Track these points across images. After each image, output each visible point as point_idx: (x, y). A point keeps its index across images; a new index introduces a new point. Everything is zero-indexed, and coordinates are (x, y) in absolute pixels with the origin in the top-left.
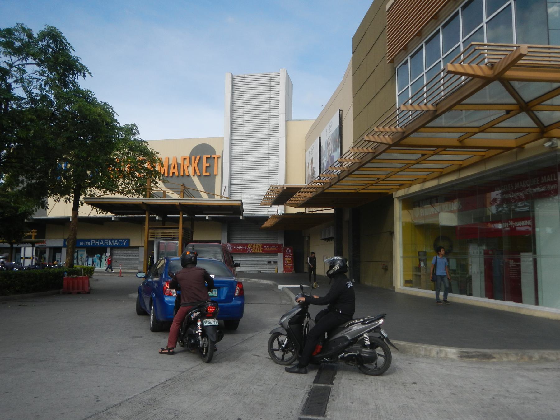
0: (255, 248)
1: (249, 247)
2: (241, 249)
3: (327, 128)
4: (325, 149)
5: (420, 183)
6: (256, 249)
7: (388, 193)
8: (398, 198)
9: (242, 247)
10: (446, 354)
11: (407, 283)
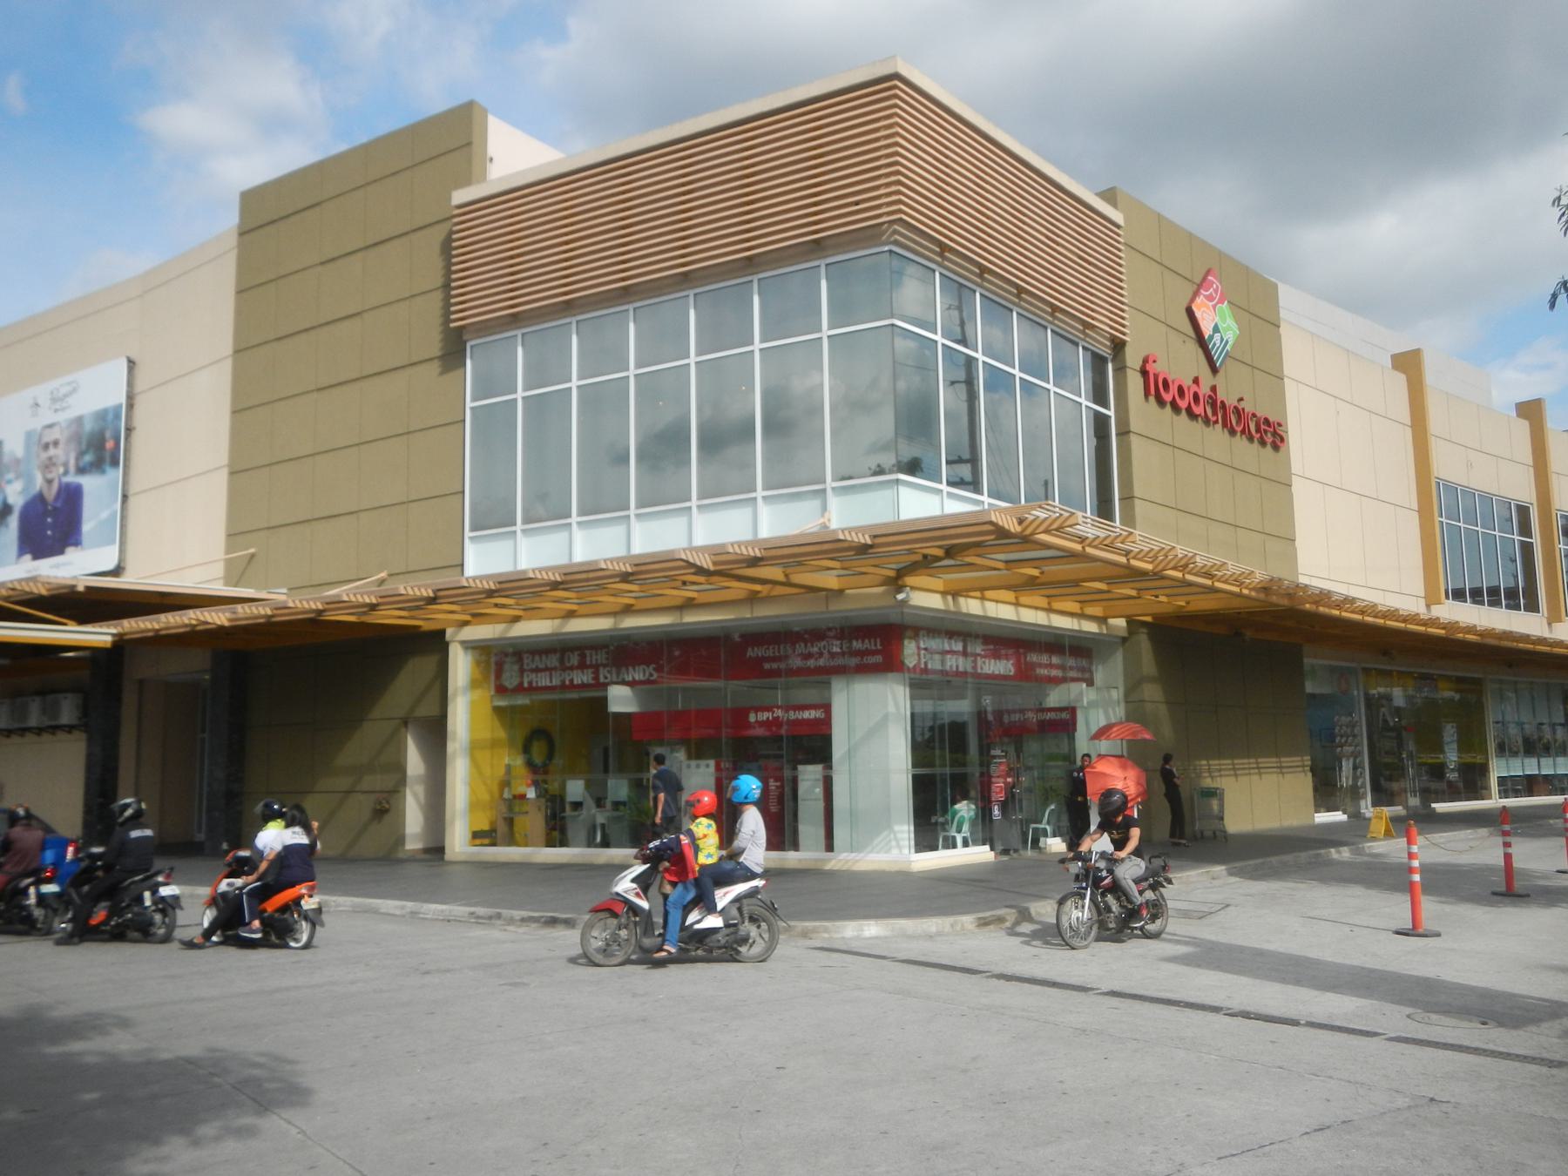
3: (41, 392)
5: (553, 618)
7: (420, 627)
10: (963, 925)
11: (476, 835)
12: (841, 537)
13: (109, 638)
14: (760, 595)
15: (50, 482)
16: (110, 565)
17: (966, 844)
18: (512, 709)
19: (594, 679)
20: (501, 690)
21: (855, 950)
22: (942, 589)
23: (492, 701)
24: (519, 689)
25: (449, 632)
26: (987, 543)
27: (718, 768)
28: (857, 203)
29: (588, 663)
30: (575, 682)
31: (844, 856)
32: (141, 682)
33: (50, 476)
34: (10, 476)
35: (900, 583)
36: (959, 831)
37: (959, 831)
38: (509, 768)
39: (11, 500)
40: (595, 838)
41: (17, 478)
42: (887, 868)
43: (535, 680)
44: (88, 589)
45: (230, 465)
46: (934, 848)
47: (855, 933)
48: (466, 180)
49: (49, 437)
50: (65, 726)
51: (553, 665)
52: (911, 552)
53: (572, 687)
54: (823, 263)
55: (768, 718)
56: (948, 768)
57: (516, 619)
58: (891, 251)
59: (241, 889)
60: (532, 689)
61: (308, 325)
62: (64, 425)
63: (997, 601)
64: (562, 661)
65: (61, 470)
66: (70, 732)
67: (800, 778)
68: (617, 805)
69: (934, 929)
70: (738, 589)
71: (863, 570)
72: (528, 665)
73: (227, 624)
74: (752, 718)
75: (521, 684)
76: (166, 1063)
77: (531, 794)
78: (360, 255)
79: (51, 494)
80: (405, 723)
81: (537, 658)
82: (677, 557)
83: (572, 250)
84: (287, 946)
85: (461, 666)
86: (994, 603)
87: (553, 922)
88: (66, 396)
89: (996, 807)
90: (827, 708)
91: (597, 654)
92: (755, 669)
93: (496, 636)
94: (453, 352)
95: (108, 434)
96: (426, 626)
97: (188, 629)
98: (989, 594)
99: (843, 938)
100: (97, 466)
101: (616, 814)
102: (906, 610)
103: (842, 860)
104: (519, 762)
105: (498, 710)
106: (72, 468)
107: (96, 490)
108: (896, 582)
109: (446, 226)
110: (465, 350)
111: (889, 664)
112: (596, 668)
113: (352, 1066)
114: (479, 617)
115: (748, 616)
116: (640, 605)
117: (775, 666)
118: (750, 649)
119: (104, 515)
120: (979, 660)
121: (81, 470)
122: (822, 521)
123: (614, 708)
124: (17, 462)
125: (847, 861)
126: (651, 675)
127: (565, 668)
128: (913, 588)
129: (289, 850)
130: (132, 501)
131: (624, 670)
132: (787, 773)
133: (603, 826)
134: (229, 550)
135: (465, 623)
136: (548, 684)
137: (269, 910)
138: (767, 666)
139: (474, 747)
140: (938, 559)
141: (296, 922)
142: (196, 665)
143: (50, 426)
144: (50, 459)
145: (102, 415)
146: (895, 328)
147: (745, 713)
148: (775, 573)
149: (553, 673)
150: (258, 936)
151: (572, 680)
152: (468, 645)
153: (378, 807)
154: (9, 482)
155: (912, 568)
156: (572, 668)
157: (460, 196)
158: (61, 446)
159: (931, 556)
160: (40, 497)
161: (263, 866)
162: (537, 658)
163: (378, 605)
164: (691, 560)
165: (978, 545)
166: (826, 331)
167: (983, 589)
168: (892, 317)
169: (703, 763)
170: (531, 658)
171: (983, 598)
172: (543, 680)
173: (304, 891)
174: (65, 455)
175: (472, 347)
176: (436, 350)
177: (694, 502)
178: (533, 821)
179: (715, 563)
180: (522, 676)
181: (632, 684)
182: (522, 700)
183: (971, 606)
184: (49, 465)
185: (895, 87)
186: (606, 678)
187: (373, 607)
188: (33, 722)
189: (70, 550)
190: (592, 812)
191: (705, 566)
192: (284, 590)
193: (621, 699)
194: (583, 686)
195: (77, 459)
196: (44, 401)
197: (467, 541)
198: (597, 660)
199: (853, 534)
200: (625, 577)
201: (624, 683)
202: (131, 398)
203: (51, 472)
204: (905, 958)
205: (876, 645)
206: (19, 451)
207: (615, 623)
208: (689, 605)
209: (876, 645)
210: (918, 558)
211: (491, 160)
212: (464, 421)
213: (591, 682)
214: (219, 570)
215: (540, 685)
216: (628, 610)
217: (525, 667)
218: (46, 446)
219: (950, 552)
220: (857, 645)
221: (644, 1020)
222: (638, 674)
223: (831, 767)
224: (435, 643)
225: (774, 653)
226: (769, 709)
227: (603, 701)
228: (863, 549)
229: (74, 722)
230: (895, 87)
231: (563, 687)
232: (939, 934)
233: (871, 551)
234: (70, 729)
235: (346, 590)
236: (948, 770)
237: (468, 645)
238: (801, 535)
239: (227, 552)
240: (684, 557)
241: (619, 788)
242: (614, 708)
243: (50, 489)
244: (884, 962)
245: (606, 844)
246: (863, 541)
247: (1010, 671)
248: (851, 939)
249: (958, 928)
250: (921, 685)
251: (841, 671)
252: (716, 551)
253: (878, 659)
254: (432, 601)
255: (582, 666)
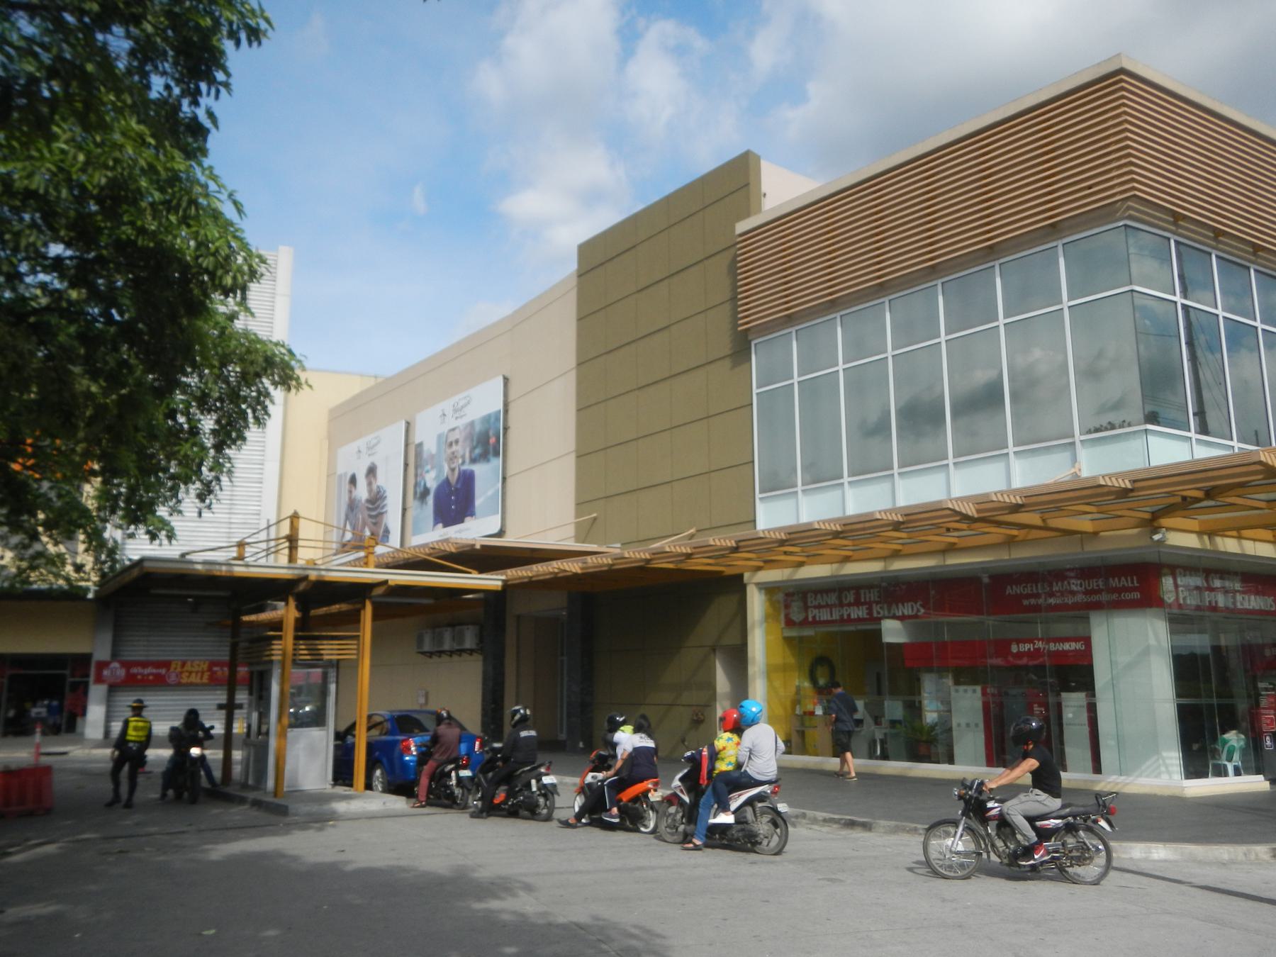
0: (190, 673)
1: (172, 670)
2: (149, 675)
3: (447, 405)
4: (434, 450)
5: (832, 563)
6: (194, 675)
8: (757, 584)
9: (154, 671)
10: (1257, 855)
12: (1102, 482)
13: (500, 583)
14: (1017, 539)
15: (453, 470)
16: (495, 529)
17: (1237, 772)
18: (801, 639)
19: (868, 614)
20: (789, 623)
21: (1146, 871)
22: (1197, 529)
23: (782, 632)
24: (805, 623)
25: (746, 576)
26: (1253, 483)
27: (984, 693)
28: (1090, 187)
29: (863, 600)
30: (852, 617)
31: (1113, 778)
32: (519, 617)
33: (453, 466)
34: (428, 467)
35: (1156, 524)
36: (1230, 760)
37: (1230, 760)
38: (798, 690)
39: (428, 485)
40: (875, 751)
41: (432, 468)
42: (1158, 792)
43: (818, 614)
44: (483, 546)
45: (577, 451)
46: (1204, 775)
47: (1143, 855)
48: (747, 214)
49: (452, 438)
50: (468, 650)
51: (833, 603)
52: (1171, 494)
53: (850, 620)
54: (1060, 243)
55: (1030, 649)
56: (1215, 700)
57: (801, 564)
58: (1126, 226)
59: (602, 781)
60: (815, 623)
61: (630, 340)
62: (461, 428)
63: (1254, 540)
64: (840, 598)
65: (460, 461)
66: (471, 654)
67: (1063, 704)
68: (893, 723)
69: (1226, 857)
70: (997, 534)
71: (1119, 513)
72: (812, 602)
73: (579, 571)
74: (1014, 649)
75: (807, 618)
76: (565, 926)
77: (819, 711)
78: (666, 282)
79: (453, 480)
80: (714, 650)
81: (819, 596)
82: (944, 507)
83: (834, 258)
84: (638, 831)
85: (756, 604)
86: (1252, 542)
87: (851, 824)
88: (462, 407)
89: (1268, 738)
90: (1087, 641)
91: (870, 593)
92: (1014, 605)
93: (785, 578)
94: (741, 350)
95: (491, 433)
96: (729, 571)
97: (552, 576)
98: (1245, 533)
99: (1131, 859)
100: (484, 457)
101: (893, 731)
102: (1162, 550)
103: (1109, 782)
104: (807, 684)
105: (788, 640)
106: (467, 460)
107: (485, 475)
108: (1152, 523)
109: (732, 251)
110: (750, 348)
111: (1148, 599)
112: (869, 605)
113: (710, 945)
114: (770, 564)
115: (1007, 557)
116: (907, 550)
117: (1033, 601)
118: (1009, 587)
119: (490, 493)
120: (1239, 597)
121: (473, 461)
122: (1073, 471)
123: (888, 638)
124: (432, 456)
125: (1117, 784)
126: (918, 611)
127: (841, 605)
128: (1168, 529)
129: (637, 751)
130: (509, 481)
131: (894, 606)
132: (1051, 699)
133: (883, 742)
134: (578, 515)
135: (759, 569)
136: (829, 618)
137: (624, 800)
138: (1026, 602)
139: (771, 671)
140: (1197, 500)
141: (645, 811)
142: (556, 604)
143: (453, 429)
144: (453, 453)
145: (487, 419)
146: (1135, 294)
147: (1008, 643)
148: (1033, 518)
149: (834, 609)
150: (617, 820)
151: (849, 615)
152: (764, 587)
153: (695, 718)
154: (428, 472)
155: (1169, 510)
156: (849, 605)
157: (741, 227)
158: (460, 443)
159: (1191, 498)
160: (447, 481)
161: (619, 764)
162: (819, 596)
163: (691, 554)
164: (957, 509)
165: (1242, 485)
166: (1066, 303)
167: (1239, 529)
168: (1131, 284)
169: (970, 688)
170: (814, 596)
171: (1240, 537)
172: (824, 615)
173: (650, 786)
174: (463, 450)
175: (756, 345)
176: (727, 351)
177: (951, 460)
178: (821, 734)
179: (978, 511)
180: (806, 611)
181: (902, 618)
182: (808, 632)
183: (1229, 545)
184: (452, 458)
185: (1122, 81)
186: (879, 613)
187: (689, 556)
188: (446, 647)
189: (468, 519)
190: (869, 727)
191: (970, 514)
192: (619, 545)
193: (893, 632)
194: (859, 620)
195: (471, 452)
196: (449, 412)
197: (757, 501)
198: (870, 598)
199: (1113, 479)
200: (897, 526)
201: (894, 617)
202: (506, 405)
203: (453, 463)
204: (1203, 884)
205: (1133, 583)
206: (434, 450)
207: (885, 567)
208: (951, 549)
209: (1133, 583)
210: (1179, 499)
211: (765, 195)
212: (752, 404)
213: (865, 616)
214: (571, 531)
215: (822, 619)
216: (896, 555)
217: (809, 604)
218: (451, 445)
219: (1210, 494)
220: (1114, 583)
221: (960, 926)
222: (907, 610)
223: (1094, 695)
224: (736, 585)
225: (1032, 590)
226: (1031, 641)
227: (878, 633)
228: (1124, 493)
229: (474, 647)
230: (1122, 81)
231: (842, 621)
232: (1233, 862)
233: (1131, 495)
234: (471, 652)
235: (667, 543)
236: (1215, 701)
237: (764, 587)
238: (1055, 483)
239: (577, 517)
240: (950, 506)
241: (894, 709)
242: (888, 638)
243: (453, 475)
244: (1183, 887)
245: (885, 757)
246: (1123, 486)
247: (1271, 606)
248: (1140, 860)
249: (1253, 857)
250: (1180, 621)
251: (1098, 606)
252: (981, 501)
253: (1137, 595)
254: (736, 550)
255: (857, 603)
